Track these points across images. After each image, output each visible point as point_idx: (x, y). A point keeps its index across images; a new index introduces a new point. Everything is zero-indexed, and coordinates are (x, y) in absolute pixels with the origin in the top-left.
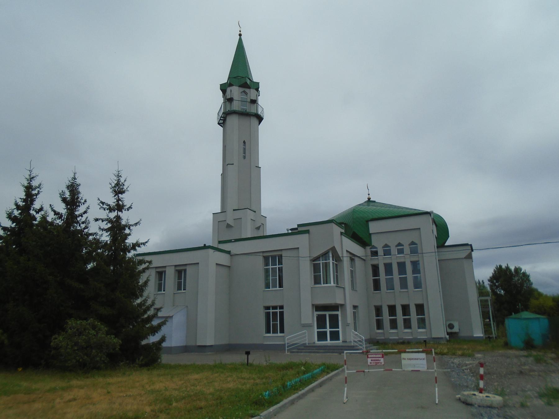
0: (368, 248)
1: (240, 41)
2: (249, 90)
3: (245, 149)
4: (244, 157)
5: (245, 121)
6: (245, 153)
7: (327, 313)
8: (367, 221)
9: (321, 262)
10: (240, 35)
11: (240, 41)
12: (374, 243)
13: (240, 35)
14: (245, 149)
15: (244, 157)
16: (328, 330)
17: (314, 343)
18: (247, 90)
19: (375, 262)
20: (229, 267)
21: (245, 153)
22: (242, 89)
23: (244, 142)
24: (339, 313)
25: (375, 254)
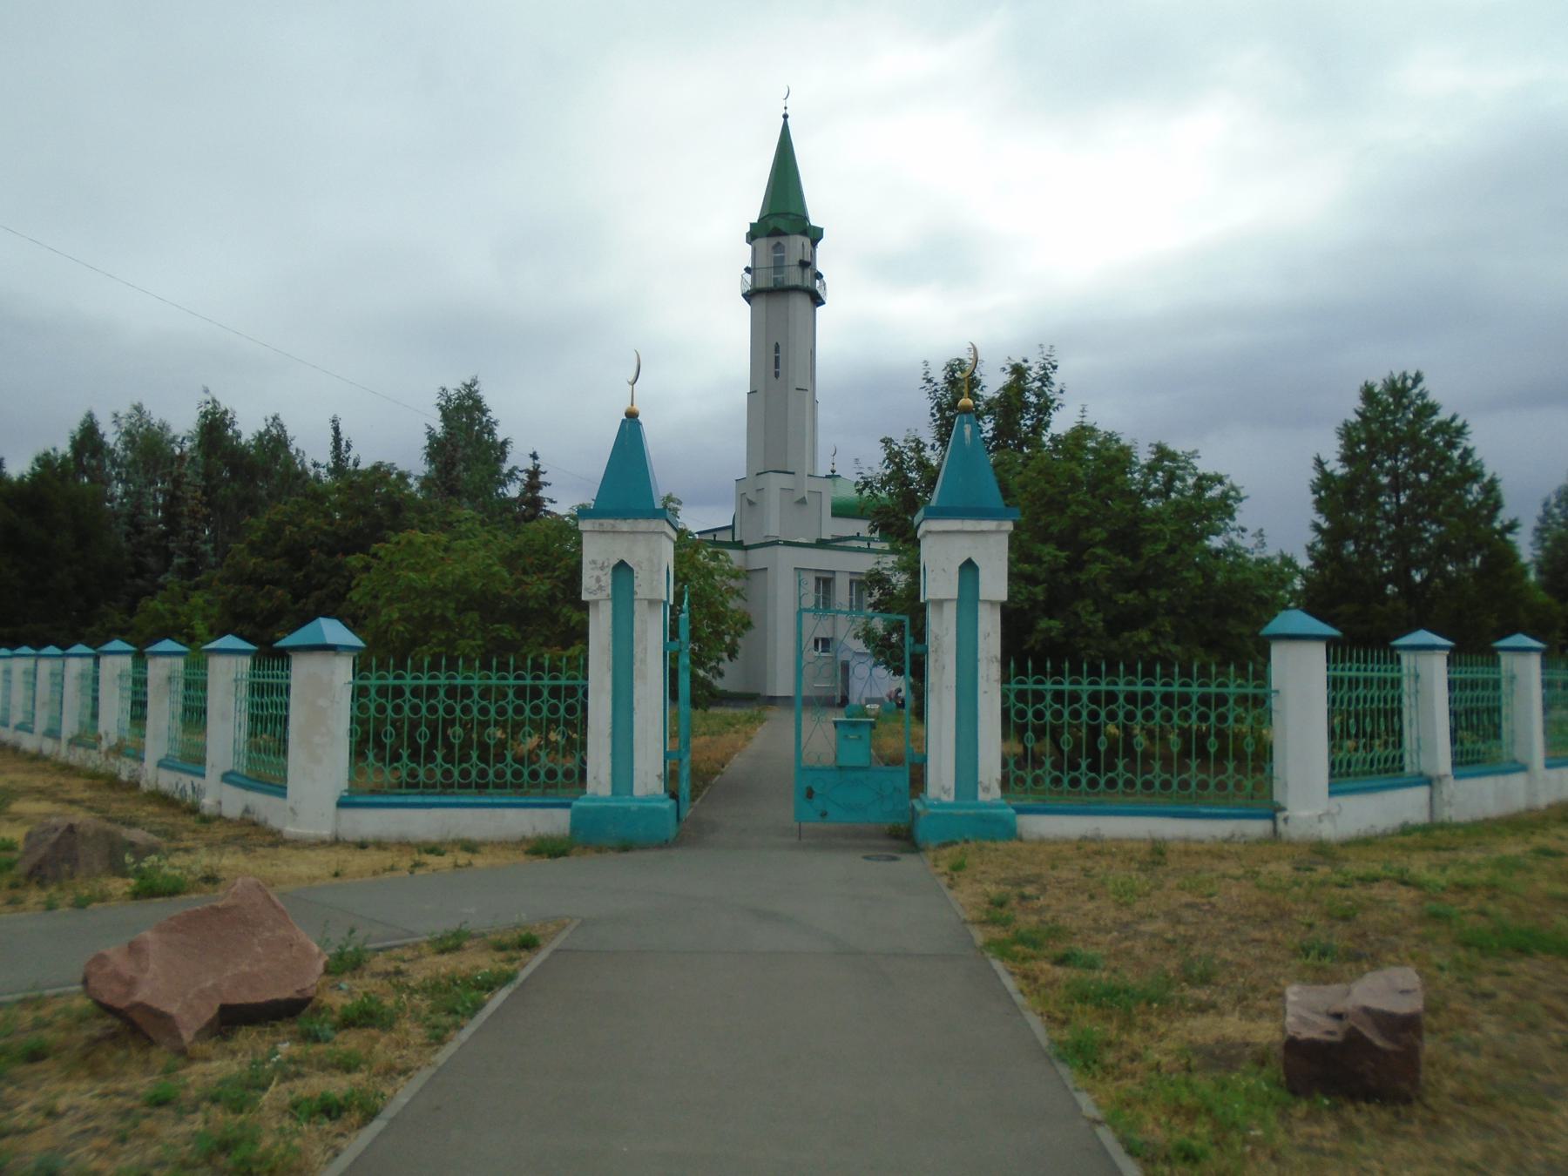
1: (785, 128)
3: (777, 359)
4: (777, 375)
6: (777, 366)
10: (786, 116)
11: (785, 128)
13: (786, 116)
14: (777, 359)
15: (777, 375)
18: (782, 240)
21: (777, 366)
22: (773, 241)
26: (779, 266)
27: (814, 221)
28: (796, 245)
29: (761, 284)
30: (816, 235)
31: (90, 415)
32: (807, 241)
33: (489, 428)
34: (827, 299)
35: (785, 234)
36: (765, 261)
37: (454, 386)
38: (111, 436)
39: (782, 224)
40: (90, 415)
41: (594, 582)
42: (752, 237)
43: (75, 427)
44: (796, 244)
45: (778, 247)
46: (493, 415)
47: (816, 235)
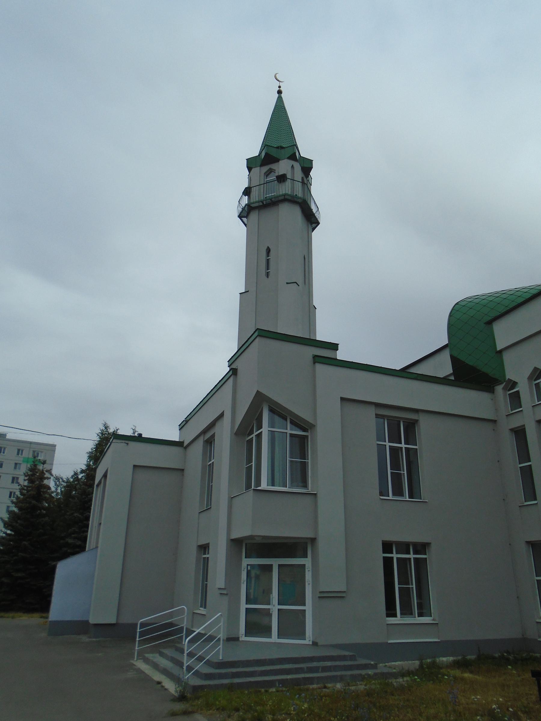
0: (499, 389)
1: (280, 100)
2: (276, 164)
3: (268, 261)
4: (268, 275)
5: (269, 215)
6: (268, 267)
7: (275, 562)
8: (490, 323)
9: (253, 436)
10: (280, 92)
11: (280, 100)
12: (510, 375)
13: (280, 92)
14: (268, 261)
15: (268, 275)
16: (274, 607)
17: (237, 639)
18: (273, 166)
19: (516, 423)
20: (183, 470)
21: (268, 267)
22: (265, 169)
23: (268, 251)
24: (307, 562)
25: (516, 399)
27: (304, 152)
28: (283, 167)
34: (321, 221)
39: (274, 153)
47: (307, 167)
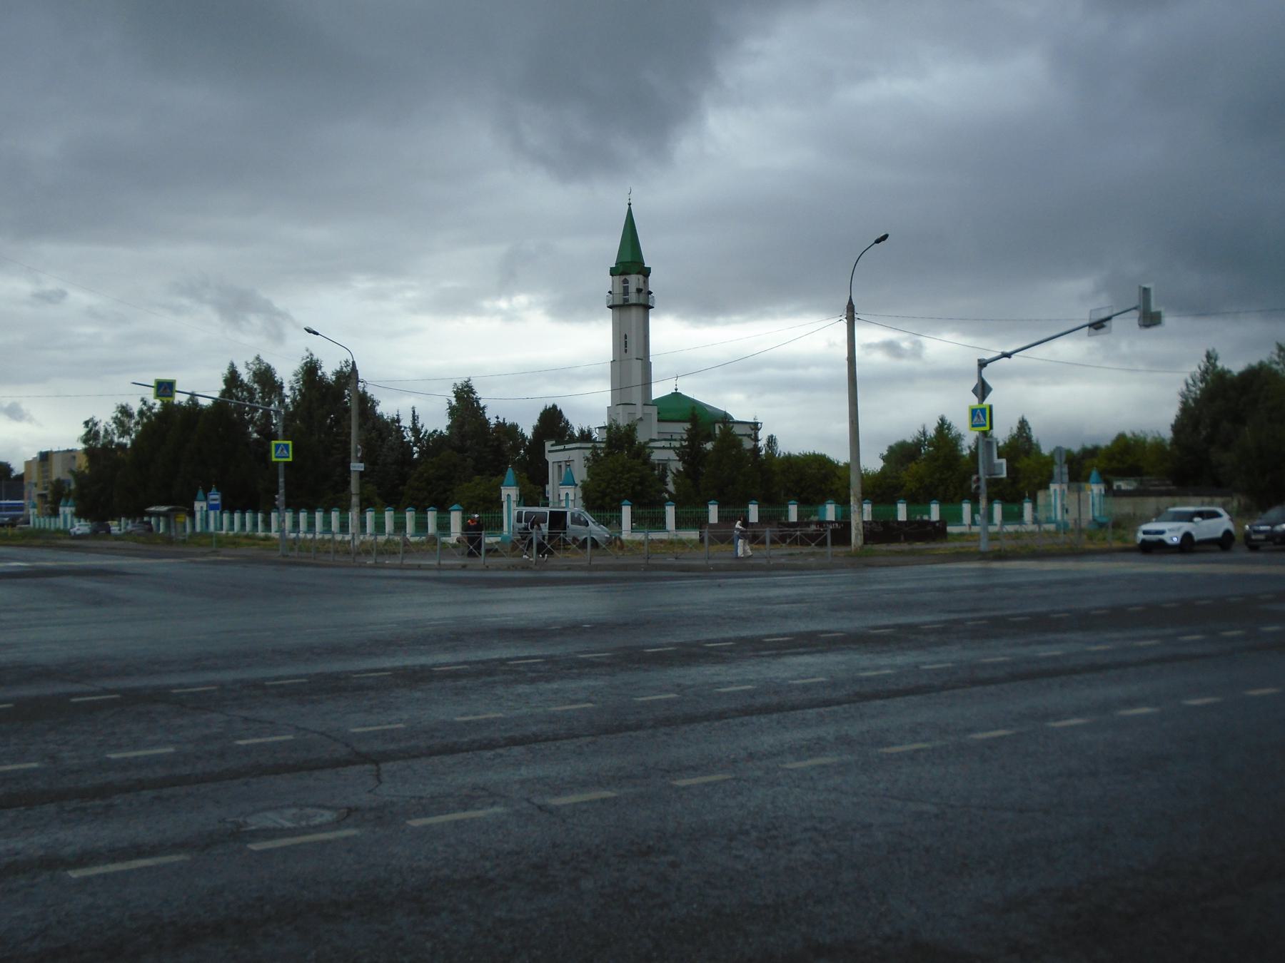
1: (630, 210)
11: (630, 210)
22: (623, 278)
26: (626, 291)
29: (617, 303)
30: (646, 272)
31: (232, 365)
32: (641, 277)
33: (477, 400)
35: (629, 274)
36: (619, 290)
37: (459, 383)
38: (245, 376)
40: (232, 365)
41: (504, 498)
42: (613, 272)
43: (226, 371)
44: (634, 281)
45: (626, 281)
46: (478, 395)
